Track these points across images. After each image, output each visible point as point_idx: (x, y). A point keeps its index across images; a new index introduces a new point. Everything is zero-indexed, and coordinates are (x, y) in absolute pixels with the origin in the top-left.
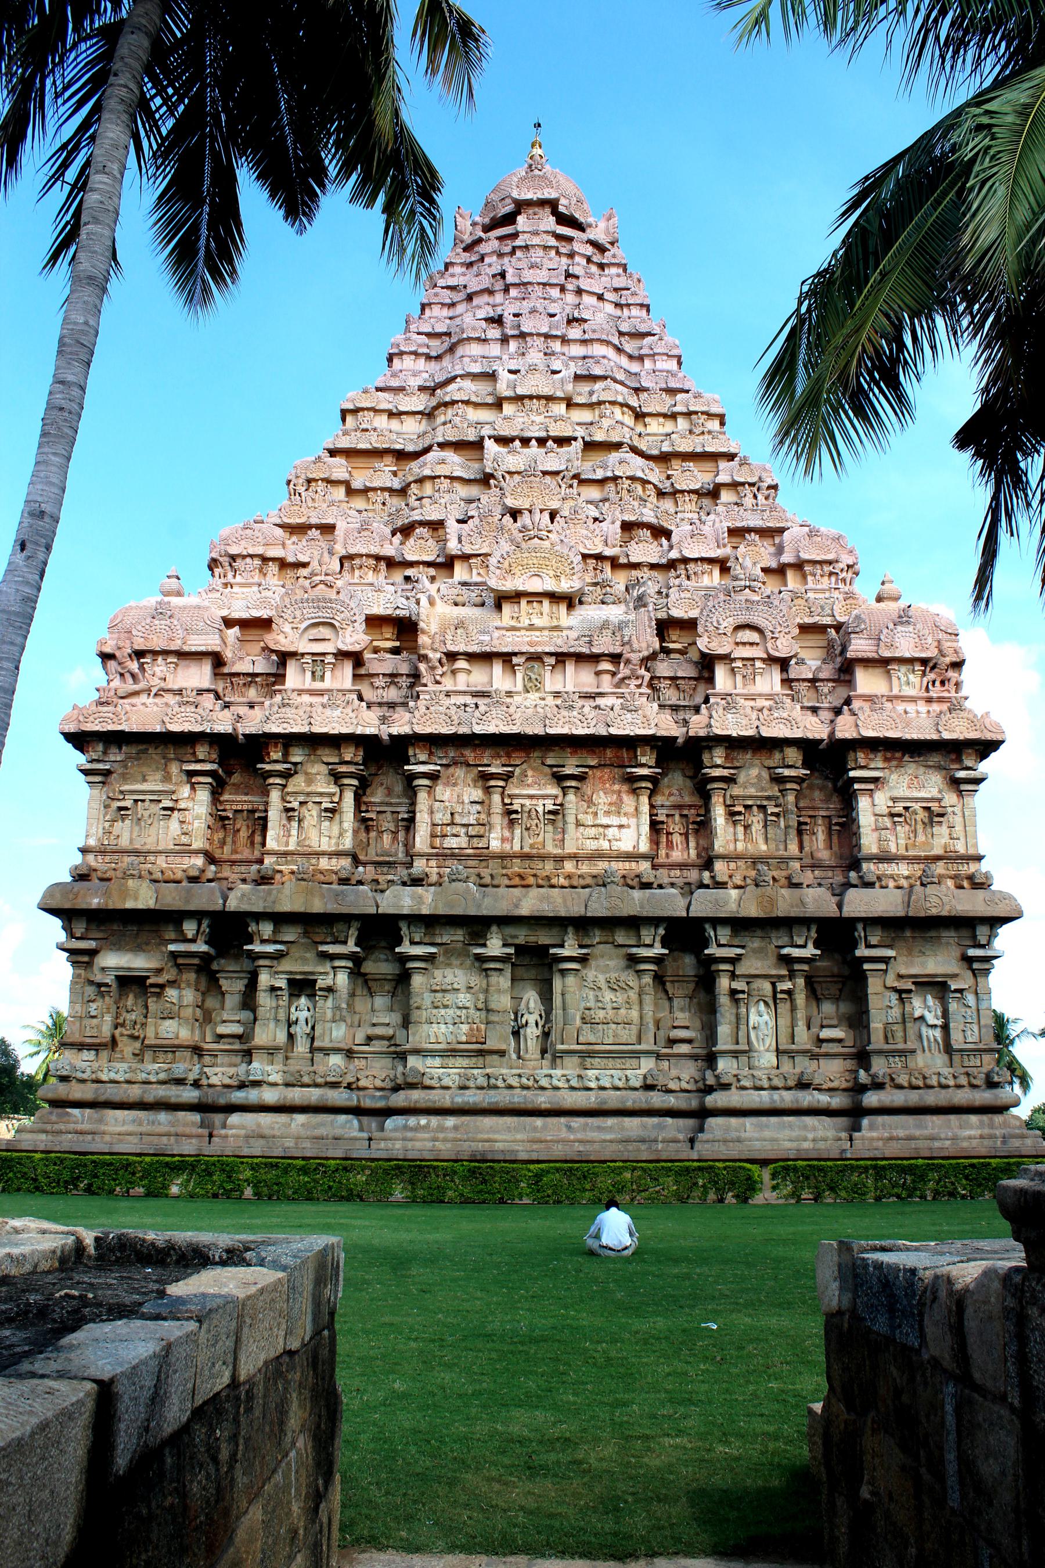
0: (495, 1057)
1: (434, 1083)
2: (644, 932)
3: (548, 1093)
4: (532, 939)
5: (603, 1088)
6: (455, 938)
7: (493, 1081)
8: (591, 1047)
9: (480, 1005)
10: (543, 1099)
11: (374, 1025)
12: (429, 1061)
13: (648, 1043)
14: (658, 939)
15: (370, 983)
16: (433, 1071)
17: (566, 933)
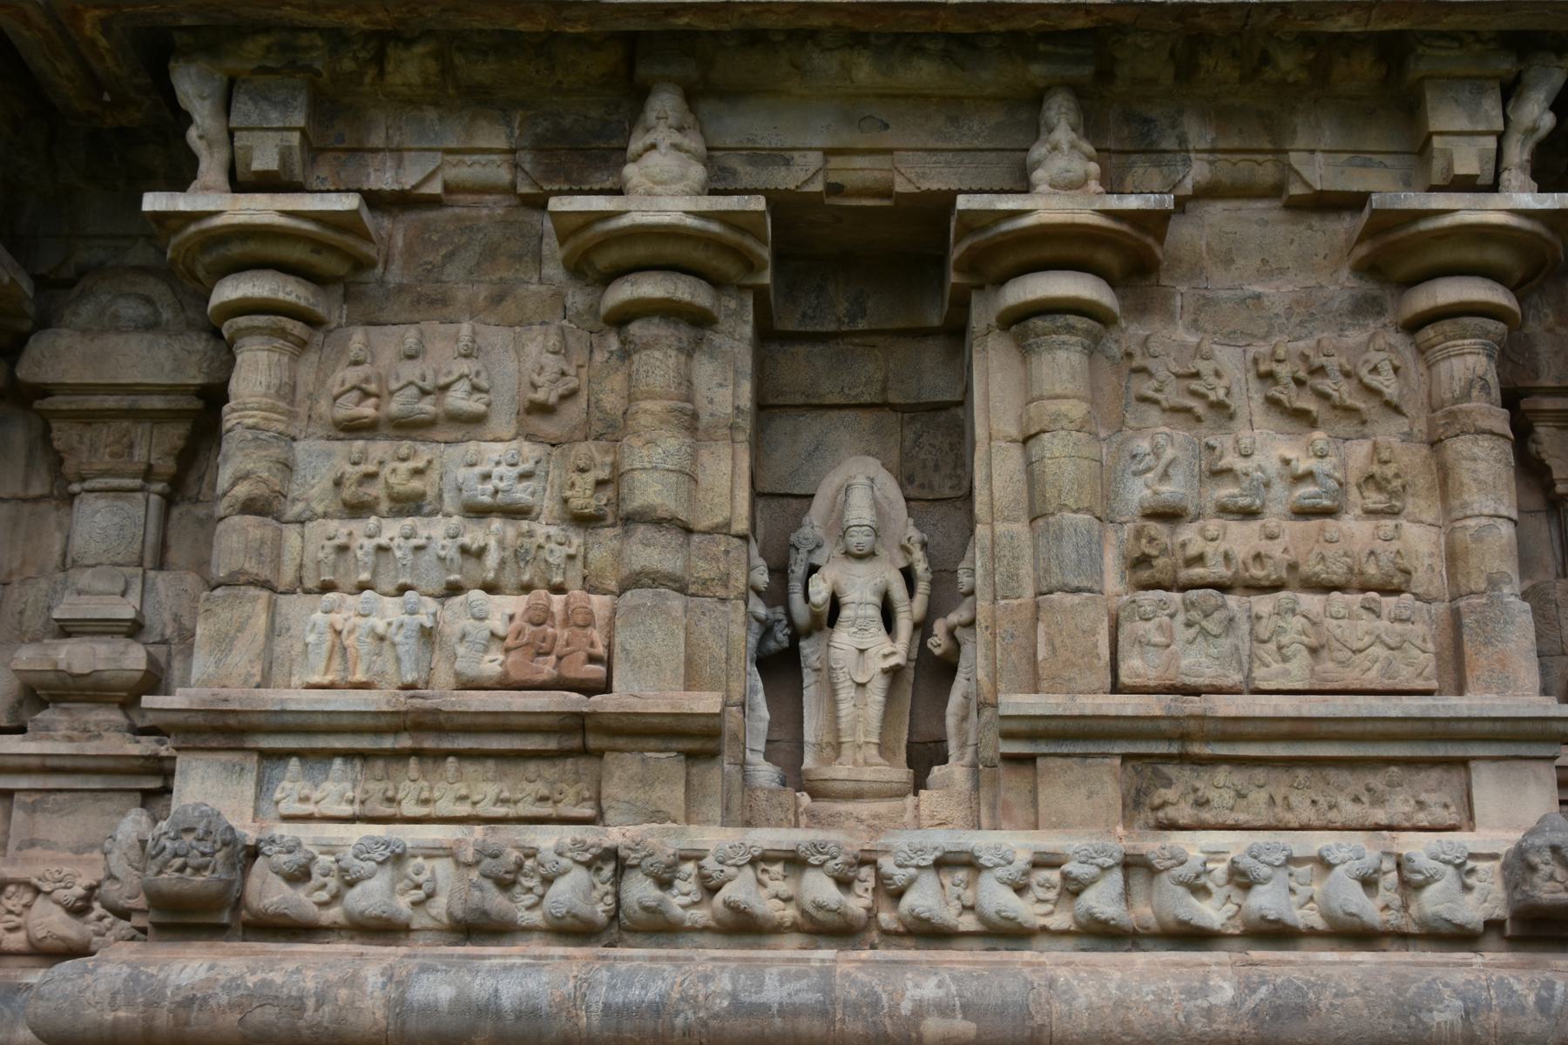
0: (666, 761)
1: (302, 901)
2: (1444, 117)
3: (956, 958)
4: (860, 171)
5: (1276, 934)
6: (466, 171)
7: (640, 890)
8: (1194, 705)
9: (583, 498)
10: (929, 989)
11: (66, 630)
12: (291, 786)
13: (1504, 686)
14: (1518, 153)
15: (63, 435)
16: (307, 834)
17: (1036, 129)
